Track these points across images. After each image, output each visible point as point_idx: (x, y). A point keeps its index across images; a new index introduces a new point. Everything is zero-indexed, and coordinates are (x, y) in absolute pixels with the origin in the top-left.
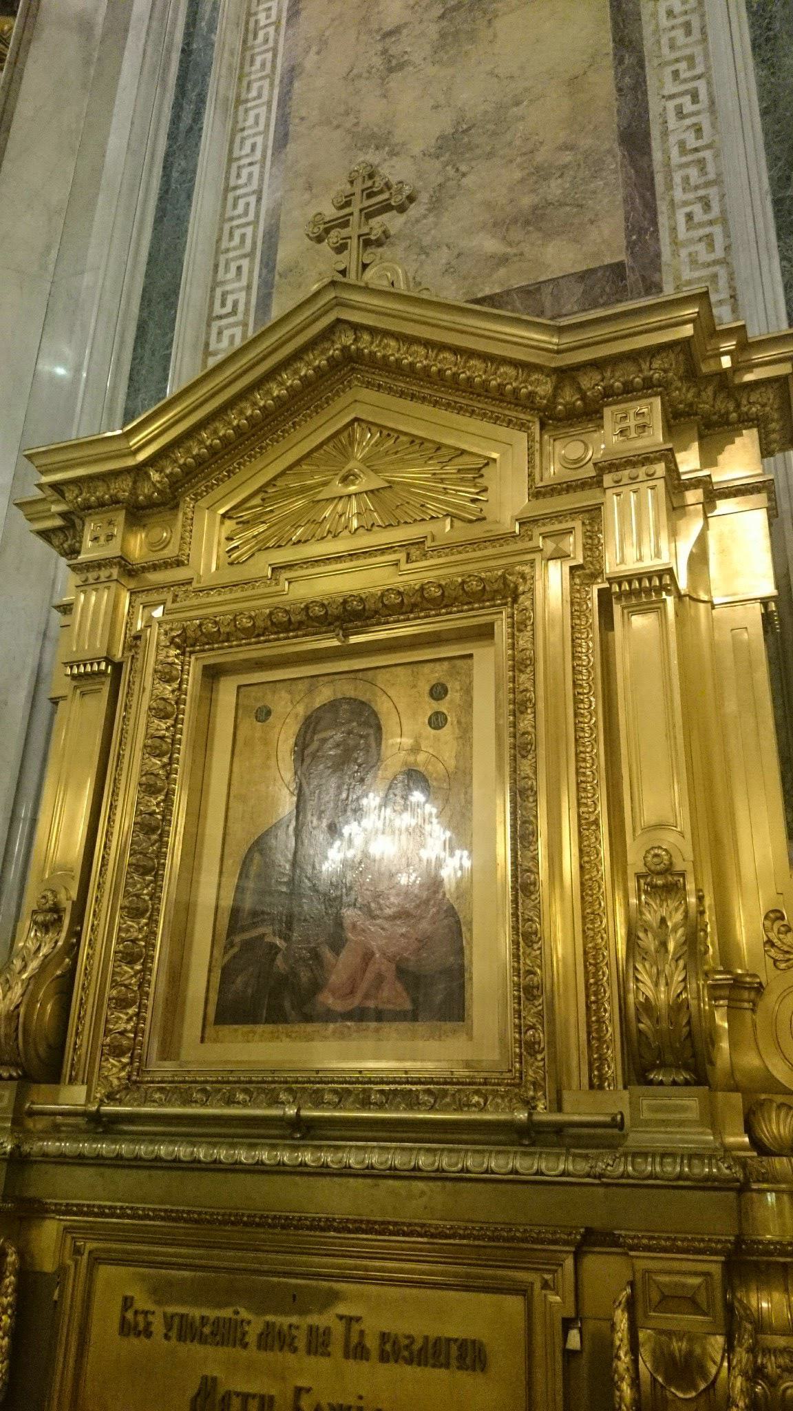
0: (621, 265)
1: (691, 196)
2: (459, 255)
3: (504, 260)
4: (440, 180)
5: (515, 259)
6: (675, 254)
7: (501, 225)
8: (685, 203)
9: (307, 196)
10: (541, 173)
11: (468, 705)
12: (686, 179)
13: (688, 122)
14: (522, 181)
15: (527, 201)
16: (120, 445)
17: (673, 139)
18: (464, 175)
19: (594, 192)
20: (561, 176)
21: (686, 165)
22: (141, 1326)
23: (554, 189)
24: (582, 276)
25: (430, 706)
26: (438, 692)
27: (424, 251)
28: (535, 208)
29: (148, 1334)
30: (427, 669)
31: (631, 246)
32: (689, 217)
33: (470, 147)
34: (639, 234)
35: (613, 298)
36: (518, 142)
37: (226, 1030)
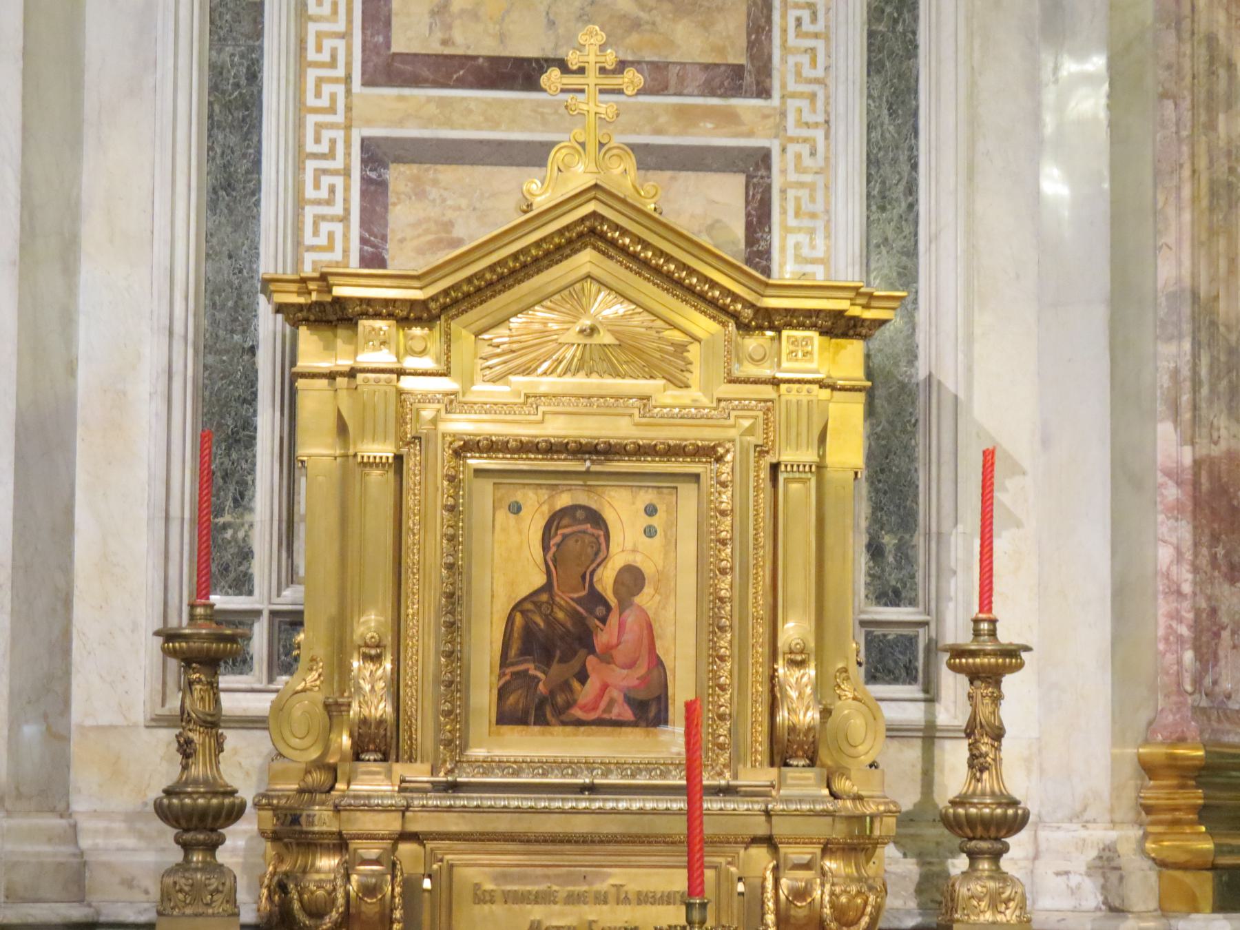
0: (741, 67)
3: (636, 25)
5: (648, 27)
6: (784, 60)
11: (673, 523)
22: (488, 898)
24: (706, 67)
25: (645, 521)
26: (651, 510)
29: (492, 902)
30: (642, 493)
31: (751, 45)
32: (799, 21)
34: (757, 33)
35: (729, 93)
37: (505, 729)
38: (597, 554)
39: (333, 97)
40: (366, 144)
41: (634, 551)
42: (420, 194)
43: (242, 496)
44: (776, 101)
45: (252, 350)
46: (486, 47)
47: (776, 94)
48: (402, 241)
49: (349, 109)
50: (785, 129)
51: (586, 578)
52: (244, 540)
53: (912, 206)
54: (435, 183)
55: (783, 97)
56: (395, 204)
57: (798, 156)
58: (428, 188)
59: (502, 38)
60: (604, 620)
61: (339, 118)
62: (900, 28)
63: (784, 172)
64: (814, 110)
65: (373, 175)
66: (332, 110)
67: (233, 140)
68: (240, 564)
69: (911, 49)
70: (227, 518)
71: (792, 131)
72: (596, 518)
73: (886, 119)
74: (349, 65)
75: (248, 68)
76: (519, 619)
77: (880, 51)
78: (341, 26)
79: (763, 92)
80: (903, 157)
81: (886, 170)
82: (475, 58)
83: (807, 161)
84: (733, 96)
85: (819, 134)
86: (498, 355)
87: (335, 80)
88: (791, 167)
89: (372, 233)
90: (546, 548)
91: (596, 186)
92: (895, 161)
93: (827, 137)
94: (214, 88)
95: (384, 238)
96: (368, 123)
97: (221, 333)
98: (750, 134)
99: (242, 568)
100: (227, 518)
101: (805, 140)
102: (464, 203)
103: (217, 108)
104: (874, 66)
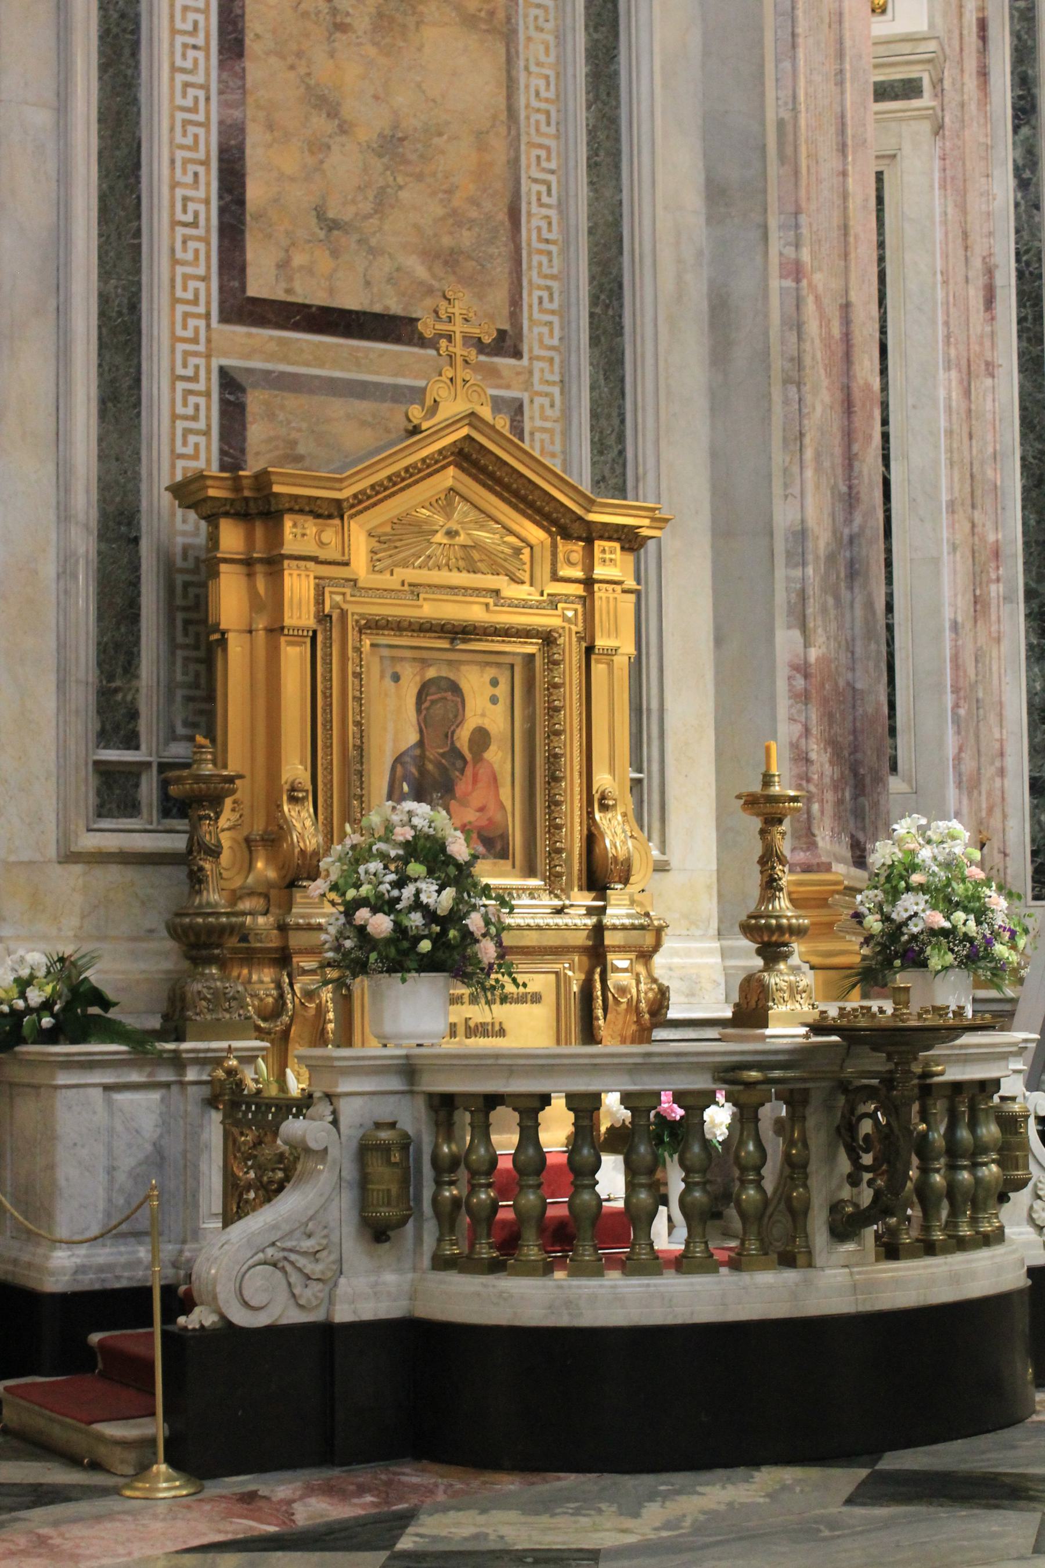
1: (542, 282)
2: (398, 270)
3: (430, 291)
4: (381, 183)
6: (530, 329)
7: (432, 255)
8: (539, 288)
9: (268, 137)
10: (456, 219)
12: (540, 264)
13: (544, 211)
14: (443, 219)
15: (447, 241)
16: (337, 485)
17: (535, 222)
18: (400, 188)
19: (491, 256)
20: (469, 229)
21: (540, 252)
23: (466, 238)
25: (490, 691)
27: (373, 251)
28: (452, 252)
32: (541, 299)
33: (406, 162)
36: (440, 175)
38: (456, 716)
39: (196, 329)
40: (223, 371)
41: (483, 715)
42: (271, 416)
43: (130, 663)
44: (525, 361)
45: (136, 540)
46: (318, 297)
47: (526, 356)
48: (257, 454)
49: (209, 341)
50: (532, 385)
51: (449, 736)
52: (132, 703)
53: (622, 452)
54: (282, 407)
55: (530, 359)
56: (252, 423)
57: (542, 407)
58: (277, 412)
59: (331, 291)
60: (462, 771)
61: (201, 348)
62: (610, 312)
63: (532, 418)
64: (552, 372)
65: (232, 398)
66: (195, 340)
67: (118, 360)
68: (129, 722)
69: (619, 330)
70: (118, 683)
71: (538, 387)
72: (455, 688)
73: (602, 382)
74: (208, 303)
75: (129, 299)
76: (399, 769)
77: (597, 329)
78: (201, 271)
79: (517, 354)
80: (615, 414)
81: (603, 422)
82: (309, 306)
83: (549, 412)
84: (497, 355)
85: (556, 391)
86: (385, 550)
87: (197, 316)
88: (537, 415)
89: (231, 447)
90: (419, 711)
91: (473, 414)
92: (609, 417)
93: (562, 393)
94: (102, 314)
95: (243, 451)
96: (225, 354)
97: (111, 524)
98: (508, 387)
99: (131, 726)
100: (118, 683)
101: (547, 395)
102: (304, 425)
103: (104, 330)
104: (594, 341)
